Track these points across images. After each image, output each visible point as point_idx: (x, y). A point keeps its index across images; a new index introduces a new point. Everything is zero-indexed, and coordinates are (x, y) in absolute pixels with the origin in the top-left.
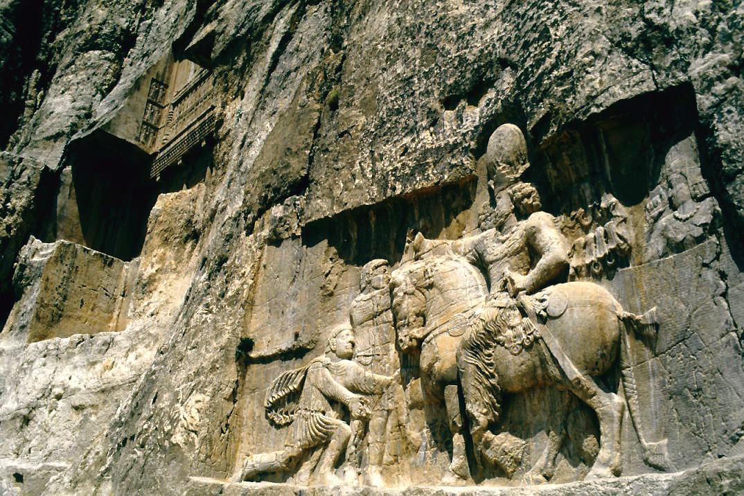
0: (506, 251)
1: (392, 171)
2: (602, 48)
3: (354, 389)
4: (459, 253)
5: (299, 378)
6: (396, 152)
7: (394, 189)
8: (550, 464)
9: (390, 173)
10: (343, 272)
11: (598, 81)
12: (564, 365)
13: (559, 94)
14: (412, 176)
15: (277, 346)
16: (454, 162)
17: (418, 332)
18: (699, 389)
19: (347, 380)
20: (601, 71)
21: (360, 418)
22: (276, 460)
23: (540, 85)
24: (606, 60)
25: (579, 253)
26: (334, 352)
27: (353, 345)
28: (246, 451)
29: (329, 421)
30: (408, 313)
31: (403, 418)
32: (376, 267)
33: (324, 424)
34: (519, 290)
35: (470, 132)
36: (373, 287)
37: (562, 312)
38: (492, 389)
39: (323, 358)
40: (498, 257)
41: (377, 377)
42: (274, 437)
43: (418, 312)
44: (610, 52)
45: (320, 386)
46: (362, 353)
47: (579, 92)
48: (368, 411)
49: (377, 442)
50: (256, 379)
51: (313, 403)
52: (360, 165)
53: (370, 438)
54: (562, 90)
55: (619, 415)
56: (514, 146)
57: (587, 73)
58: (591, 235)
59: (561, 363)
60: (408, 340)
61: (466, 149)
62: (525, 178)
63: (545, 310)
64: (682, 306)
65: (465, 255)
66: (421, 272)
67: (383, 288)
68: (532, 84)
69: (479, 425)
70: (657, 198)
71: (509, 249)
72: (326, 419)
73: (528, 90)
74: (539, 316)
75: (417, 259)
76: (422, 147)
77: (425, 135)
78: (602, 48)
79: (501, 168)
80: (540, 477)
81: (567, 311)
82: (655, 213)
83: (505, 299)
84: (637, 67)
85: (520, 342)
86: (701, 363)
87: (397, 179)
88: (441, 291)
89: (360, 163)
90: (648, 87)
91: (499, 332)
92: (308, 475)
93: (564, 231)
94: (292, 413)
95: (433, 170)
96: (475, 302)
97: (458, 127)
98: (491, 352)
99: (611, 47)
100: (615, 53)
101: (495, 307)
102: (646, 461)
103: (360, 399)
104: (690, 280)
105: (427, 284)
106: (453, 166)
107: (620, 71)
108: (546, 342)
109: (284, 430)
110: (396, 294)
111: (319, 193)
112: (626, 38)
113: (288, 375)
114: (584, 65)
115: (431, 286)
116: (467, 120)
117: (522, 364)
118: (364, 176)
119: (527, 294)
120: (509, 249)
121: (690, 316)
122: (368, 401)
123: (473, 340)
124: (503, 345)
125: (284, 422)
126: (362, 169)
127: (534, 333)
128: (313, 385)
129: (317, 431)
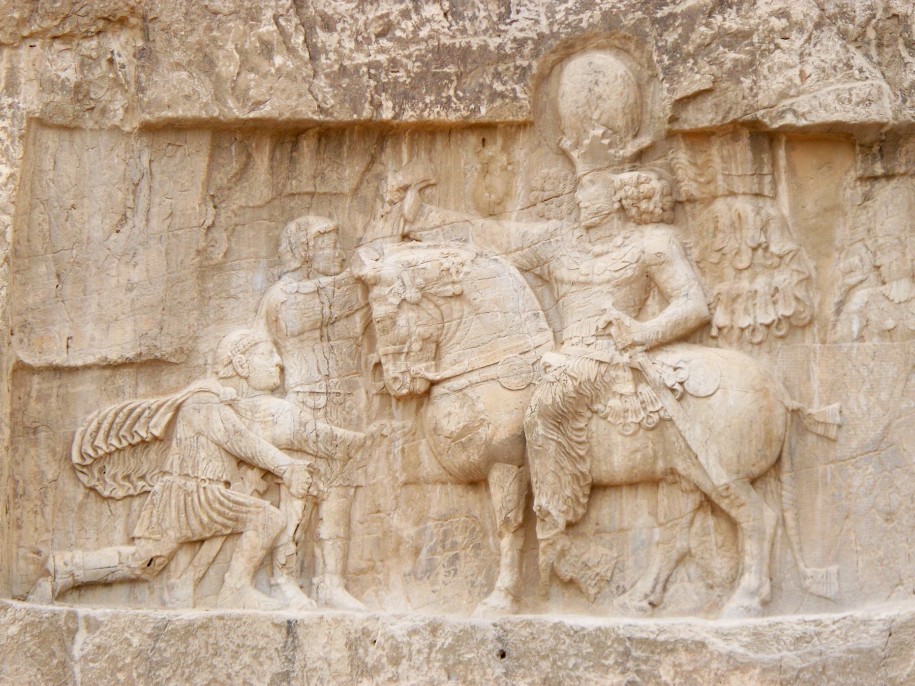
0: (607, 275)
1: (370, 65)
2: (806, 15)
3: (291, 449)
4: (497, 247)
5: (165, 414)
6: (365, 24)
7: (378, 106)
8: (659, 587)
9: (365, 69)
10: (236, 225)
11: (796, 71)
12: (708, 464)
13: (729, 65)
14: (413, 88)
15: (94, 350)
16: (498, 87)
17: (427, 369)
18: (890, 514)
19: (278, 431)
20: (801, 55)
21: (306, 496)
22: (120, 563)
23: (690, 28)
24: (810, 38)
25: (726, 308)
26: (246, 378)
27: (282, 370)
28: (34, 544)
29: (241, 500)
30: (409, 335)
31: (387, 502)
32: (322, 234)
33: (231, 505)
34: (634, 345)
35: (530, 42)
36: (318, 271)
37: (710, 393)
38: (576, 478)
39: (210, 382)
40: (589, 278)
41: (339, 432)
42: (95, 520)
43: (427, 335)
44: (818, 26)
45: (220, 436)
46: (307, 388)
47: (765, 77)
48: (321, 486)
49: (338, 537)
50: (39, 407)
51: (203, 465)
52: (277, 23)
53: (326, 530)
54: (736, 60)
55: (772, 531)
56: (626, 103)
57: (777, 47)
58: (745, 285)
59: (702, 459)
60: (408, 380)
61: (524, 71)
62: (640, 157)
63: (681, 384)
64: (878, 410)
65: (507, 253)
66: (433, 271)
67: (337, 274)
68: (673, 16)
69: (556, 527)
70: (855, 260)
71: (617, 275)
72: (234, 494)
73: (665, 24)
74: (673, 390)
75: (405, 237)
76: (430, 37)
77: (431, 10)
78: (806, 15)
79: (599, 131)
80: (645, 604)
81: (719, 393)
82: (852, 280)
83: (604, 350)
84: (861, 71)
85: (638, 421)
86: (898, 483)
87: (381, 88)
88: (476, 311)
89: (276, 18)
90: (878, 114)
91: (597, 396)
92: (190, 590)
93: (701, 265)
94: (143, 478)
95: (456, 90)
96: (538, 339)
97: (502, 17)
98: (582, 425)
99: (821, 17)
100: (824, 28)
101: (592, 359)
102: (805, 590)
103: (309, 466)
104: (895, 380)
105: (450, 294)
106: (495, 95)
107: (835, 68)
108: (680, 428)
109: (119, 509)
110: (383, 299)
111: (178, 56)
112: (844, 14)
113: (132, 411)
114: (772, 31)
115: (458, 296)
116: (518, 12)
117: (636, 451)
118: (291, 50)
119: (646, 351)
120: (617, 275)
121: (889, 424)
122: (322, 470)
123: (558, 406)
124: (605, 418)
125: (120, 493)
126: (282, 31)
127: (662, 413)
128: (199, 433)
129: (215, 516)
